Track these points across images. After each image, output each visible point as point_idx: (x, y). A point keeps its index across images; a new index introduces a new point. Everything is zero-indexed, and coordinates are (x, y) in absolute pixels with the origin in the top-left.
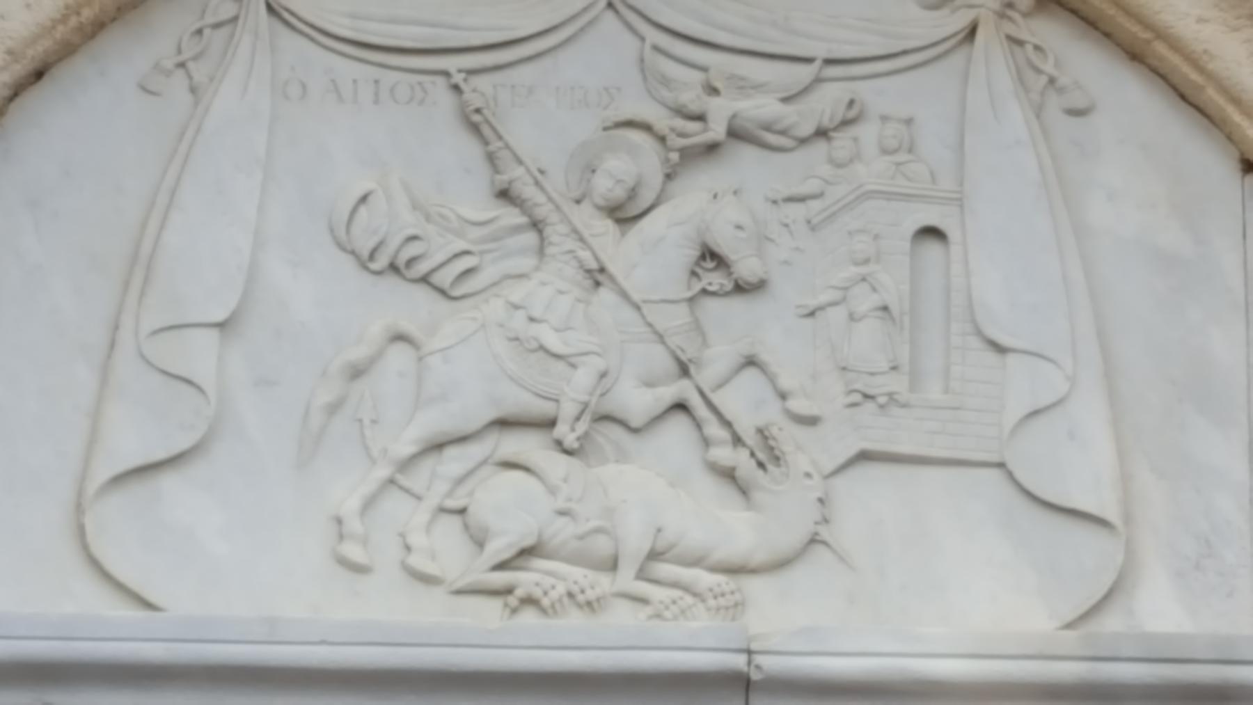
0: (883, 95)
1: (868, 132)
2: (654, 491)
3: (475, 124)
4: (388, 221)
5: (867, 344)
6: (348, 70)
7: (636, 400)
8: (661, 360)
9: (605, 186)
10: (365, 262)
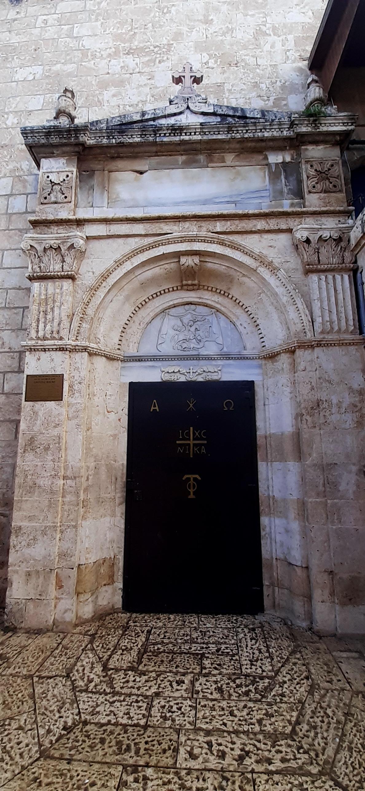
0: (207, 318)
4: (176, 327)
5: (207, 334)
6: (173, 318)
9: (190, 324)
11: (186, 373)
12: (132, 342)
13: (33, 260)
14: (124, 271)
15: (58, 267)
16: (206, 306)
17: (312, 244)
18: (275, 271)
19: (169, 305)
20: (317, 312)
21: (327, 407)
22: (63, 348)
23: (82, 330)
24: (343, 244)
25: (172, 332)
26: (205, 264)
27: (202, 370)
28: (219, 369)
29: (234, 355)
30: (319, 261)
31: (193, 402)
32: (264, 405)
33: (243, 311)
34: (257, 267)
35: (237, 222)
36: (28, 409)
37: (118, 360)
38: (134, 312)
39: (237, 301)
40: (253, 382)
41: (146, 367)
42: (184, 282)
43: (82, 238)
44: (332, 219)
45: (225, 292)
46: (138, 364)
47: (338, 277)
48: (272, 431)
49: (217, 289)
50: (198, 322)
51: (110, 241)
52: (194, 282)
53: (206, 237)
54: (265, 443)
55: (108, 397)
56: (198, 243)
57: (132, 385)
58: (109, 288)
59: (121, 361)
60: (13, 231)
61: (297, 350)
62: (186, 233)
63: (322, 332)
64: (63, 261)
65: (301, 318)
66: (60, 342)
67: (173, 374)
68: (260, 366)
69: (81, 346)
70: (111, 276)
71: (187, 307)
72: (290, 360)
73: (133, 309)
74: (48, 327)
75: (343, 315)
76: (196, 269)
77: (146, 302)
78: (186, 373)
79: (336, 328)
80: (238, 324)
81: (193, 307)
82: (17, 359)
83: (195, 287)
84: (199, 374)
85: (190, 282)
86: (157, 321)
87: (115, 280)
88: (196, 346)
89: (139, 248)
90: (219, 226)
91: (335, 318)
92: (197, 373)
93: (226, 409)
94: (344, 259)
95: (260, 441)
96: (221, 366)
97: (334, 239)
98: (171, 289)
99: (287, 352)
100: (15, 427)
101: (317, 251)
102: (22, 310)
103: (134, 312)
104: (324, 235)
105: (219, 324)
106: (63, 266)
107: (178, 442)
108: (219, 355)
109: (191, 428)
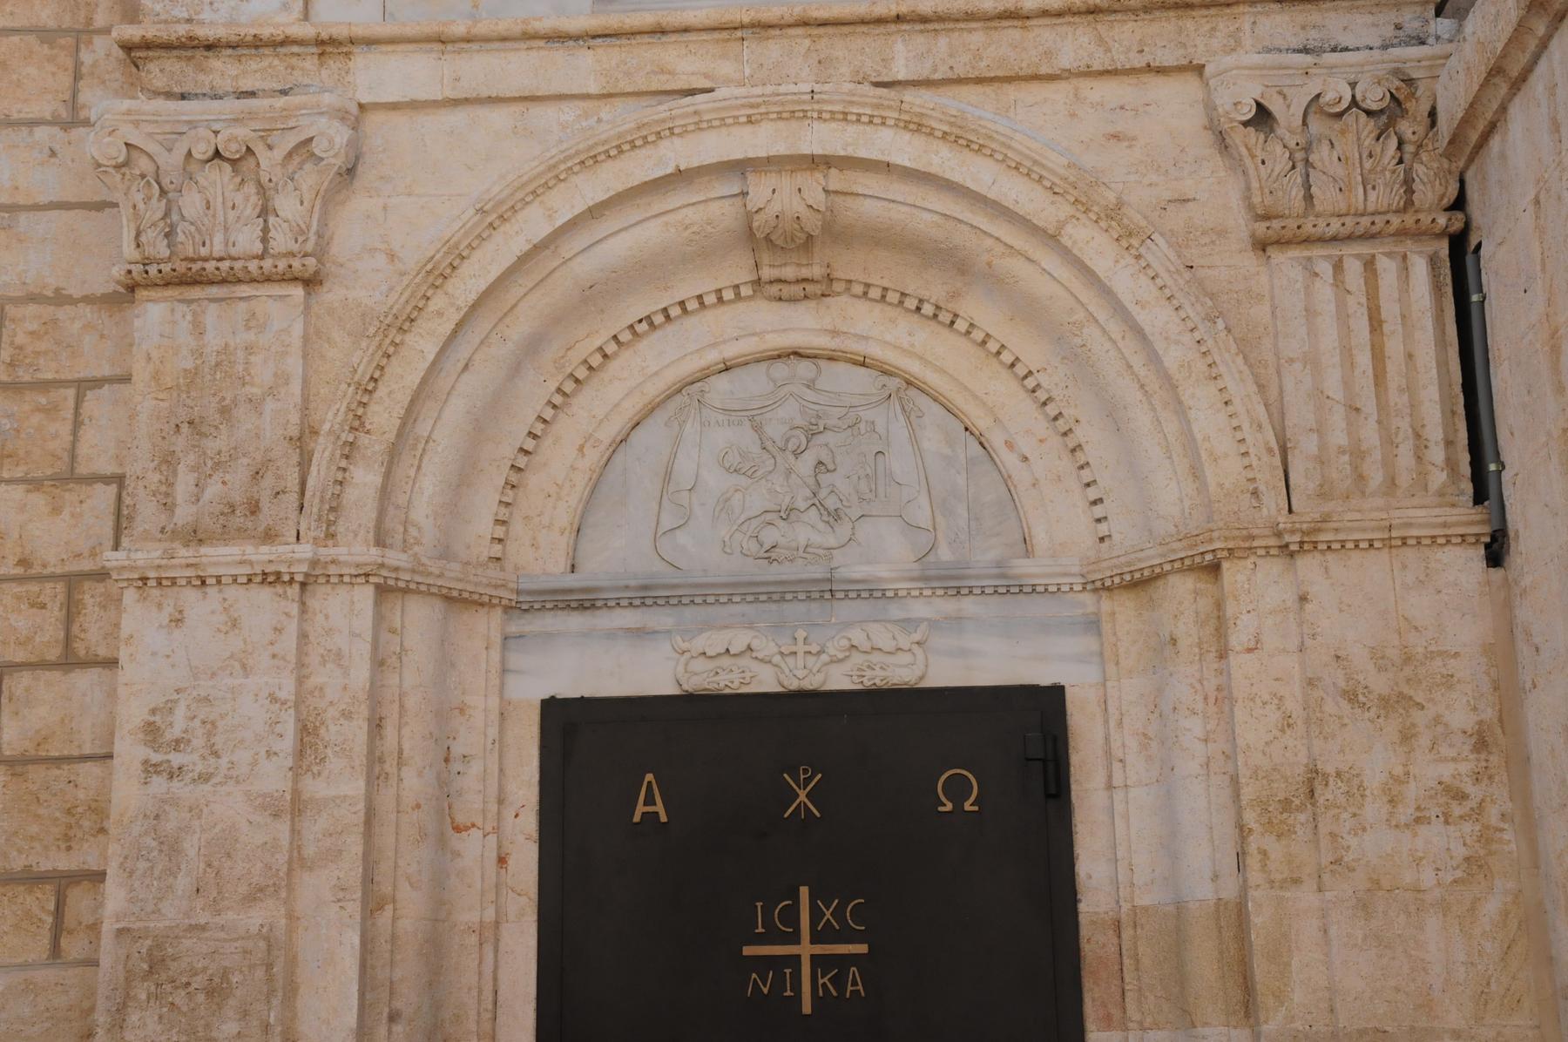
0: (867, 415)
1: (862, 426)
2: (808, 532)
3: (758, 429)
6: (721, 417)
7: (802, 505)
8: (808, 493)
9: (791, 446)
10: (727, 470)
11: (777, 659)
12: (549, 527)
13: (141, 206)
14: (519, 246)
15: (247, 240)
16: (863, 365)
17: (1280, 131)
18: (1135, 242)
19: (703, 363)
20: (1300, 415)
21: (1342, 800)
22: (278, 574)
23: (351, 495)
24: (1405, 127)
25: (715, 481)
26: (849, 201)
27: (845, 643)
28: (917, 637)
29: (978, 577)
30: (1309, 197)
31: (807, 781)
32: (1110, 786)
33: (1014, 385)
34: (1061, 225)
35: (977, 37)
36: (136, 830)
37: (494, 606)
38: (558, 400)
39: (993, 347)
40: (1057, 692)
41: (611, 635)
42: (767, 273)
43: (342, 115)
44: (1369, 19)
45: (938, 307)
46: (576, 621)
47: (1387, 268)
48: (1144, 900)
49: (903, 294)
50: (829, 433)
51: (458, 117)
52: (805, 272)
53: (851, 103)
54: (1113, 949)
55: (456, 766)
56: (816, 124)
57: (552, 709)
58: (457, 317)
59: (507, 609)
60: (15, 39)
61: (1225, 565)
62: (769, 89)
63: (1324, 494)
64: (265, 212)
65: (1239, 436)
66: (264, 549)
67: (726, 662)
68: (1093, 625)
69: (346, 564)
70: (466, 269)
71: (780, 370)
72: (1205, 604)
73: (553, 386)
74: (213, 490)
75: (1404, 424)
76: (813, 224)
77: (605, 356)
78: (777, 659)
79: (1376, 478)
80: (996, 440)
81: (804, 368)
82: (55, 612)
83: (810, 288)
84: (835, 661)
85: (789, 272)
86: (652, 436)
87: (483, 287)
88: (816, 539)
89: (577, 153)
90: (904, 56)
91: (1370, 434)
92: (824, 658)
93: (949, 807)
94: (1410, 191)
95: (1094, 942)
96: (924, 626)
97: (1369, 113)
98: (710, 299)
99: (1191, 569)
100: (52, 906)
101: (1301, 157)
102: (71, 393)
103: (558, 400)
104: (1329, 97)
105: (914, 439)
106: (266, 230)
107: (748, 951)
108: (913, 579)
109: (804, 891)
